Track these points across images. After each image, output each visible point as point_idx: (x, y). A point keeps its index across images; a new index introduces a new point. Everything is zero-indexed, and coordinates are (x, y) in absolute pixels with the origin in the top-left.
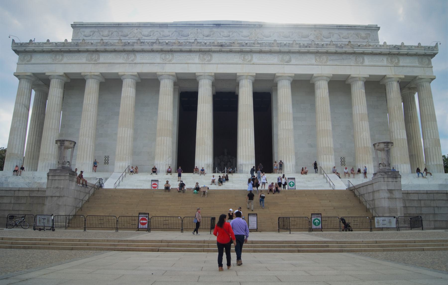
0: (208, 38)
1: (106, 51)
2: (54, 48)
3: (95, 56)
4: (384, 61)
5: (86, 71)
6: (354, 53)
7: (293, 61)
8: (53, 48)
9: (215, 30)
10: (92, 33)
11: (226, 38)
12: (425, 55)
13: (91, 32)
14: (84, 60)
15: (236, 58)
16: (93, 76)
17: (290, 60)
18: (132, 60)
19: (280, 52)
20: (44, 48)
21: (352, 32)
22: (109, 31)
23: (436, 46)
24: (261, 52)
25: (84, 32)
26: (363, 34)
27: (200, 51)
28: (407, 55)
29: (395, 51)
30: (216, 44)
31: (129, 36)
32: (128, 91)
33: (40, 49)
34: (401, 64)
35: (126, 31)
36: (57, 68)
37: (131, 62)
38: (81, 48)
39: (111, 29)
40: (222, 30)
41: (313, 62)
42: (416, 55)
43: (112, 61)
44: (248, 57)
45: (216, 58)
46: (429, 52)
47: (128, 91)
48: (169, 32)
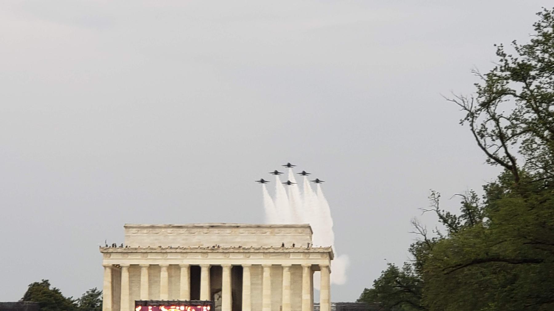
3: (145, 255)
4: (302, 256)
7: (251, 257)
12: (324, 253)
15: (221, 256)
19: (244, 252)
21: (293, 229)
26: (300, 230)
30: (210, 248)
32: (164, 274)
34: (310, 258)
35: (158, 230)
36: (125, 262)
41: (262, 257)
42: (319, 252)
44: (227, 255)
45: (210, 256)
47: (164, 274)
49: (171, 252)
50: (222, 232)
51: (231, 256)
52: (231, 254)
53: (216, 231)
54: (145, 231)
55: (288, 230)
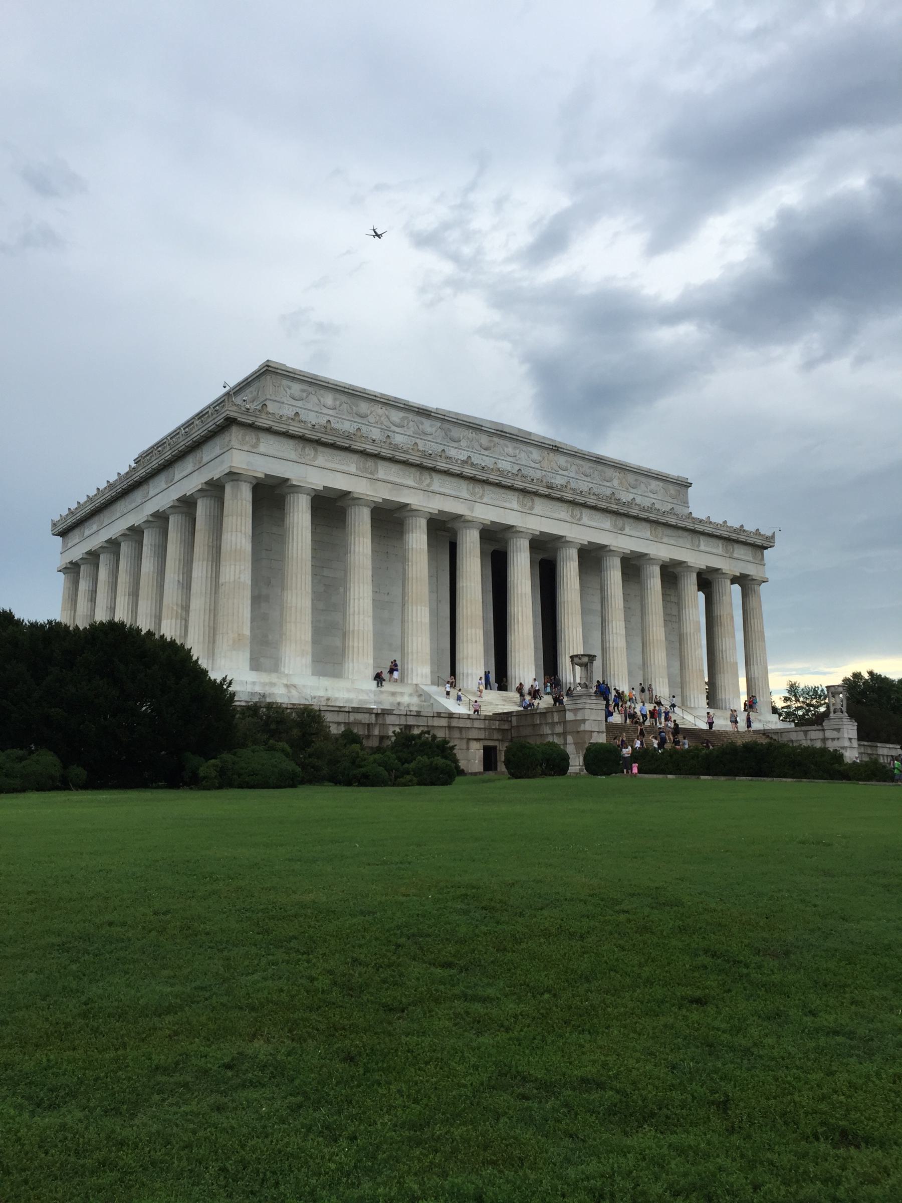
0: (486, 453)
1: (392, 460)
2: (309, 434)
3: (370, 463)
4: (718, 548)
5: (357, 490)
6: (694, 532)
7: (627, 530)
8: (306, 432)
9: (496, 439)
10: (305, 394)
11: (511, 459)
13: (303, 391)
14: (353, 469)
16: (367, 503)
17: (622, 529)
18: (428, 485)
20: (291, 428)
21: (661, 484)
22: (335, 399)
23: (773, 536)
24: (595, 508)
25: (290, 388)
26: (672, 489)
27: (524, 492)
28: (745, 543)
29: (734, 536)
30: (544, 484)
31: (371, 419)
33: (283, 428)
35: (364, 407)
37: (426, 488)
38: (357, 446)
39: (338, 396)
40: (505, 442)
41: (648, 534)
43: (397, 480)
44: (577, 511)
45: (540, 506)
46: (766, 544)
48: (431, 426)
49: (447, 473)
50: (523, 455)
51: (587, 517)
52: (586, 513)
53: (510, 448)
54: (329, 399)
55: (654, 484)
